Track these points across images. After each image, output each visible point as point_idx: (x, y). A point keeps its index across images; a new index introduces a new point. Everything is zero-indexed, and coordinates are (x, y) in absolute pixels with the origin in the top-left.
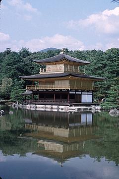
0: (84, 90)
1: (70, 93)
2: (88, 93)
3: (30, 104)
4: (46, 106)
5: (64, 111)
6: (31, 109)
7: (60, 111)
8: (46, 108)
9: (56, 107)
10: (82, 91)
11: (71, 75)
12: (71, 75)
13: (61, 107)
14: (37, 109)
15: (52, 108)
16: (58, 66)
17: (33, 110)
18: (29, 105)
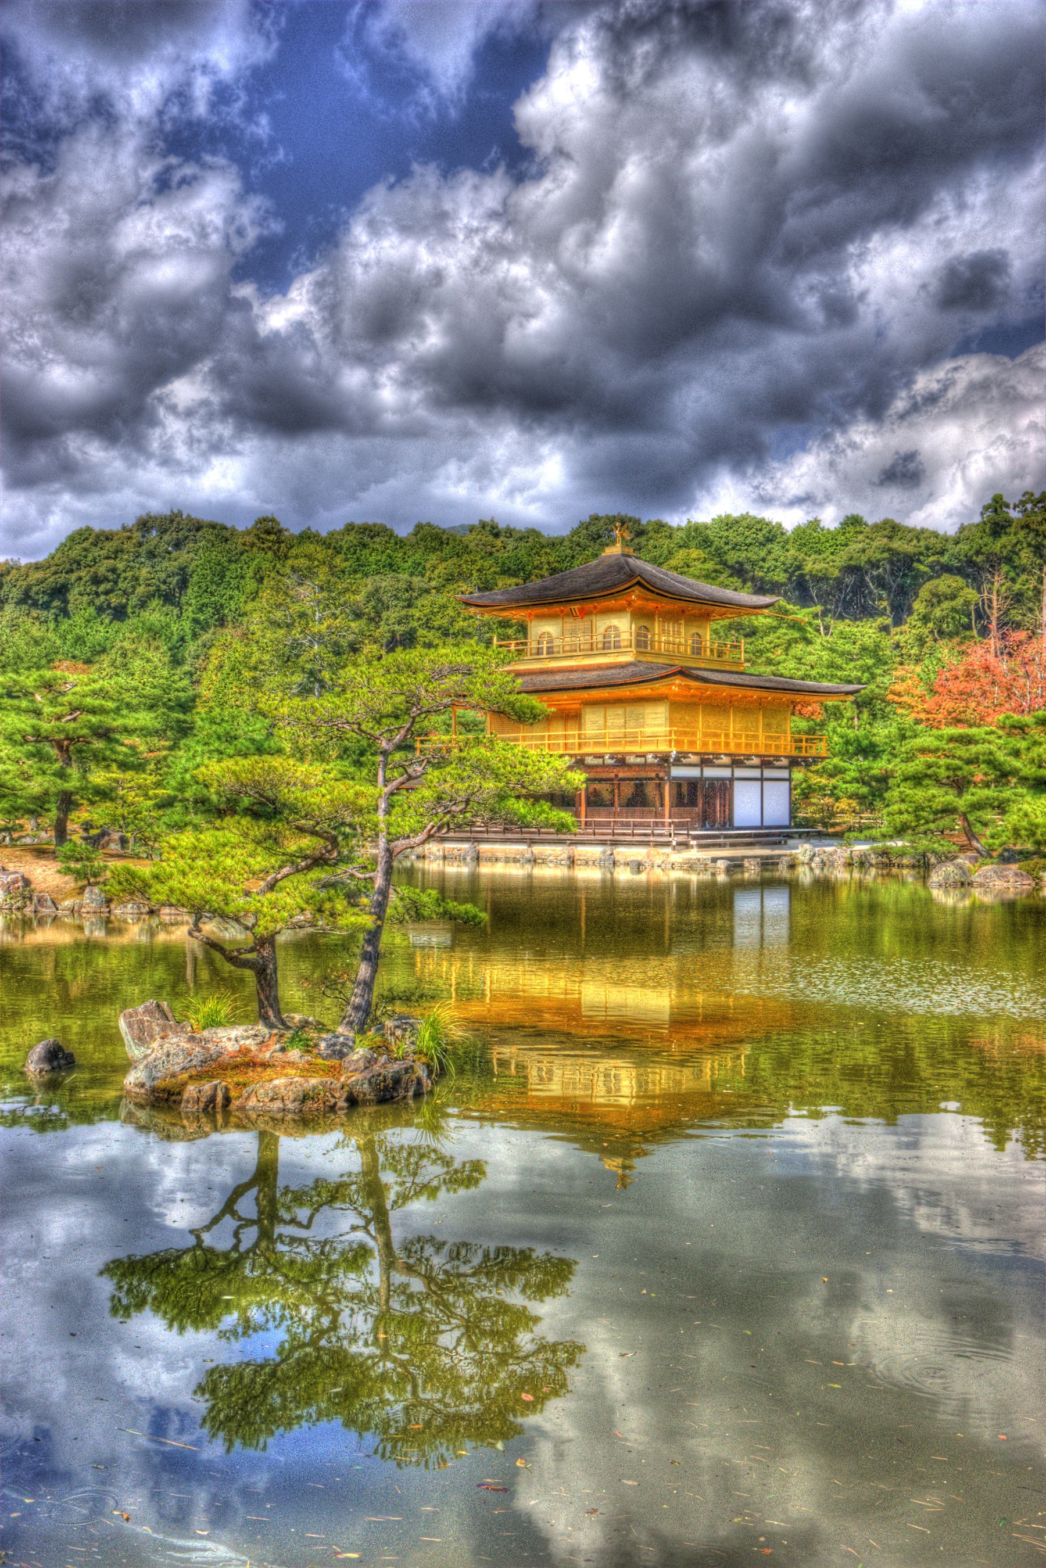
0: (748, 757)
1: (677, 772)
2: (768, 773)
3: (443, 840)
4: (537, 849)
5: (643, 877)
6: (451, 869)
7: (624, 875)
8: (534, 861)
9: (595, 851)
10: (737, 762)
11: (683, 673)
12: (683, 673)
13: (624, 853)
14: (485, 869)
15: (572, 862)
16: (602, 624)
17: (459, 876)
18: (434, 848)
